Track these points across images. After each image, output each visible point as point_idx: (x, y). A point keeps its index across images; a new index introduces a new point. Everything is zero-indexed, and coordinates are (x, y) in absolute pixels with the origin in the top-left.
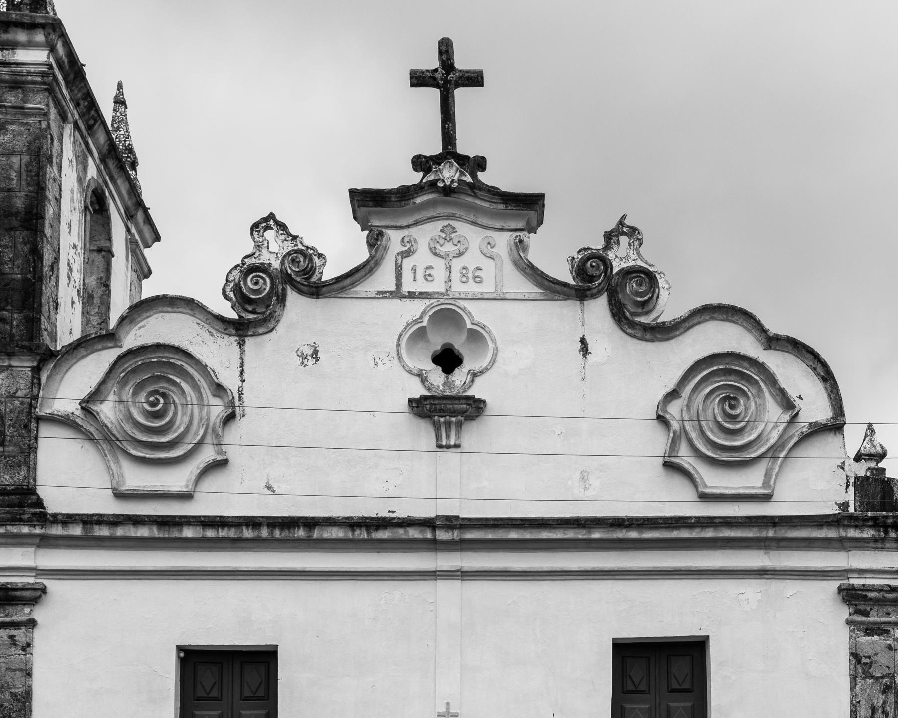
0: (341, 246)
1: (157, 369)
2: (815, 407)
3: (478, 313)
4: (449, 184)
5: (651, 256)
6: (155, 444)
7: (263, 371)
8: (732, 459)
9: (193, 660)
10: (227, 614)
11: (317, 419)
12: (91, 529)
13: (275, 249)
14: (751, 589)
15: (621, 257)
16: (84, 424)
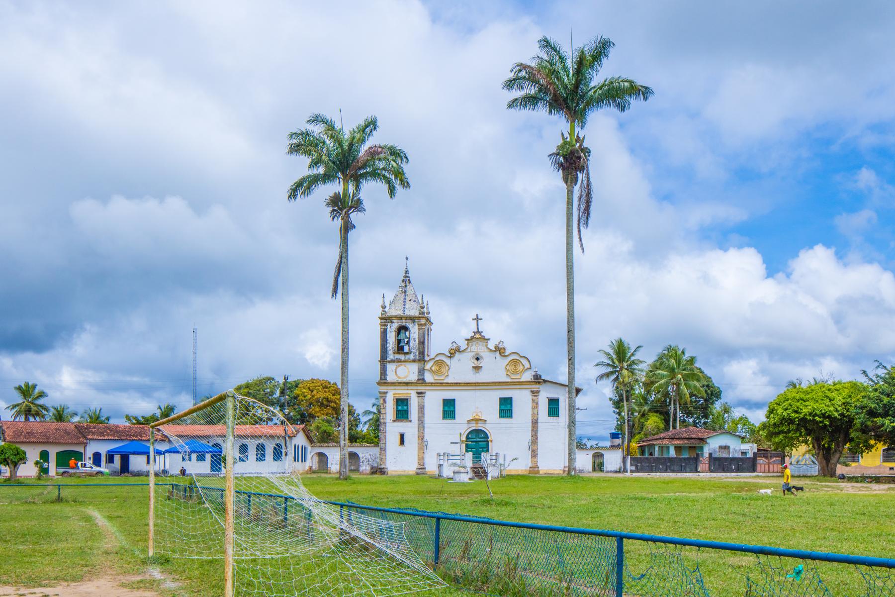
0: (463, 345)
1: (440, 363)
2: (527, 366)
3: (482, 354)
4: (478, 337)
5: (505, 345)
6: (438, 372)
7: (454, 363)
8: (516, 373)
9: (444, 400)
10: (449, 395)
11: (460, 369)
12: (432, 384)
13: (455, 345)
14: (518, 392)
15: (501, 346)
16: (430, 370)
